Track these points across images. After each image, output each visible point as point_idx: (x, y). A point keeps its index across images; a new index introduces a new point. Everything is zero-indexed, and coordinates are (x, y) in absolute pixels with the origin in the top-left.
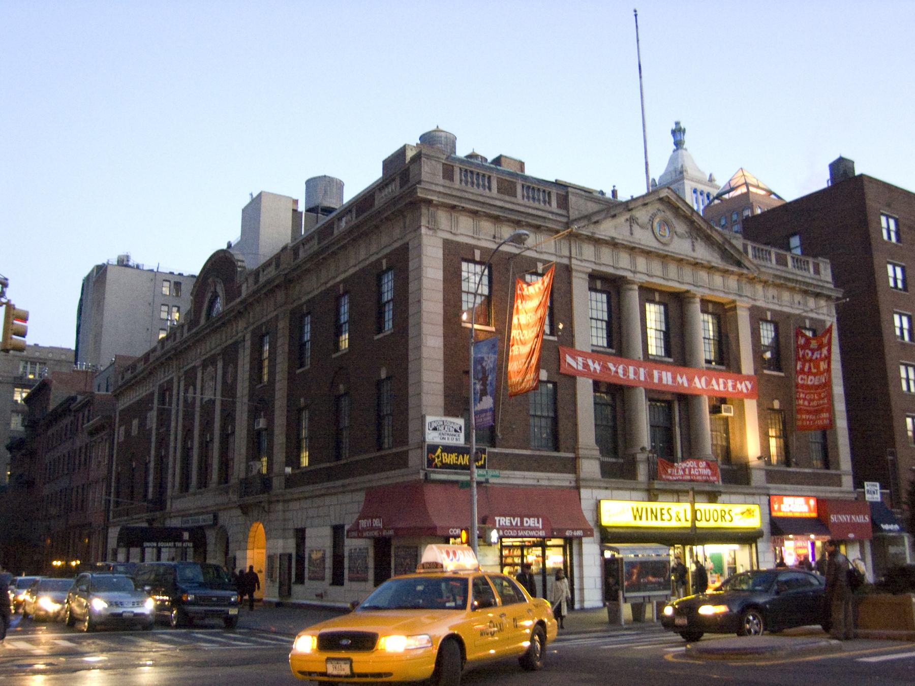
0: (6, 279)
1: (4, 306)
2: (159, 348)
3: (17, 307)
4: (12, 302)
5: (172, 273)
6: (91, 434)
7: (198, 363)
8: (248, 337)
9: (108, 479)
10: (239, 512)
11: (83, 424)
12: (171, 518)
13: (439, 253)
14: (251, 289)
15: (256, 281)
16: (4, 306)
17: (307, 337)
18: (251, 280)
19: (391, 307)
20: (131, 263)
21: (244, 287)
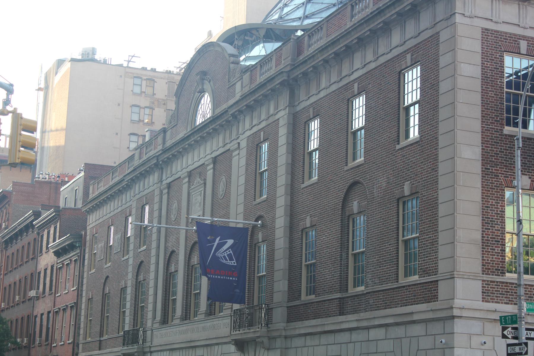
0: (12, 85)
1: (10, 115)
2: (137, 157)
3: (24, 116)
4: (18, 112)
5: (144, 69)
6: (58, 254)
7: (183, 173)
8: (244, 144)
9: (76, 306)
10: (233, 348)
11: (48, 243)
12: (151, 352)
13: (477, 46)
14: (246, 90)
15: (252, 80)
16: (10, 115)
17: (314, 144)
18: (246, 76)
19: (417, 111)
20: (97, 57)
21: (238, 86)
